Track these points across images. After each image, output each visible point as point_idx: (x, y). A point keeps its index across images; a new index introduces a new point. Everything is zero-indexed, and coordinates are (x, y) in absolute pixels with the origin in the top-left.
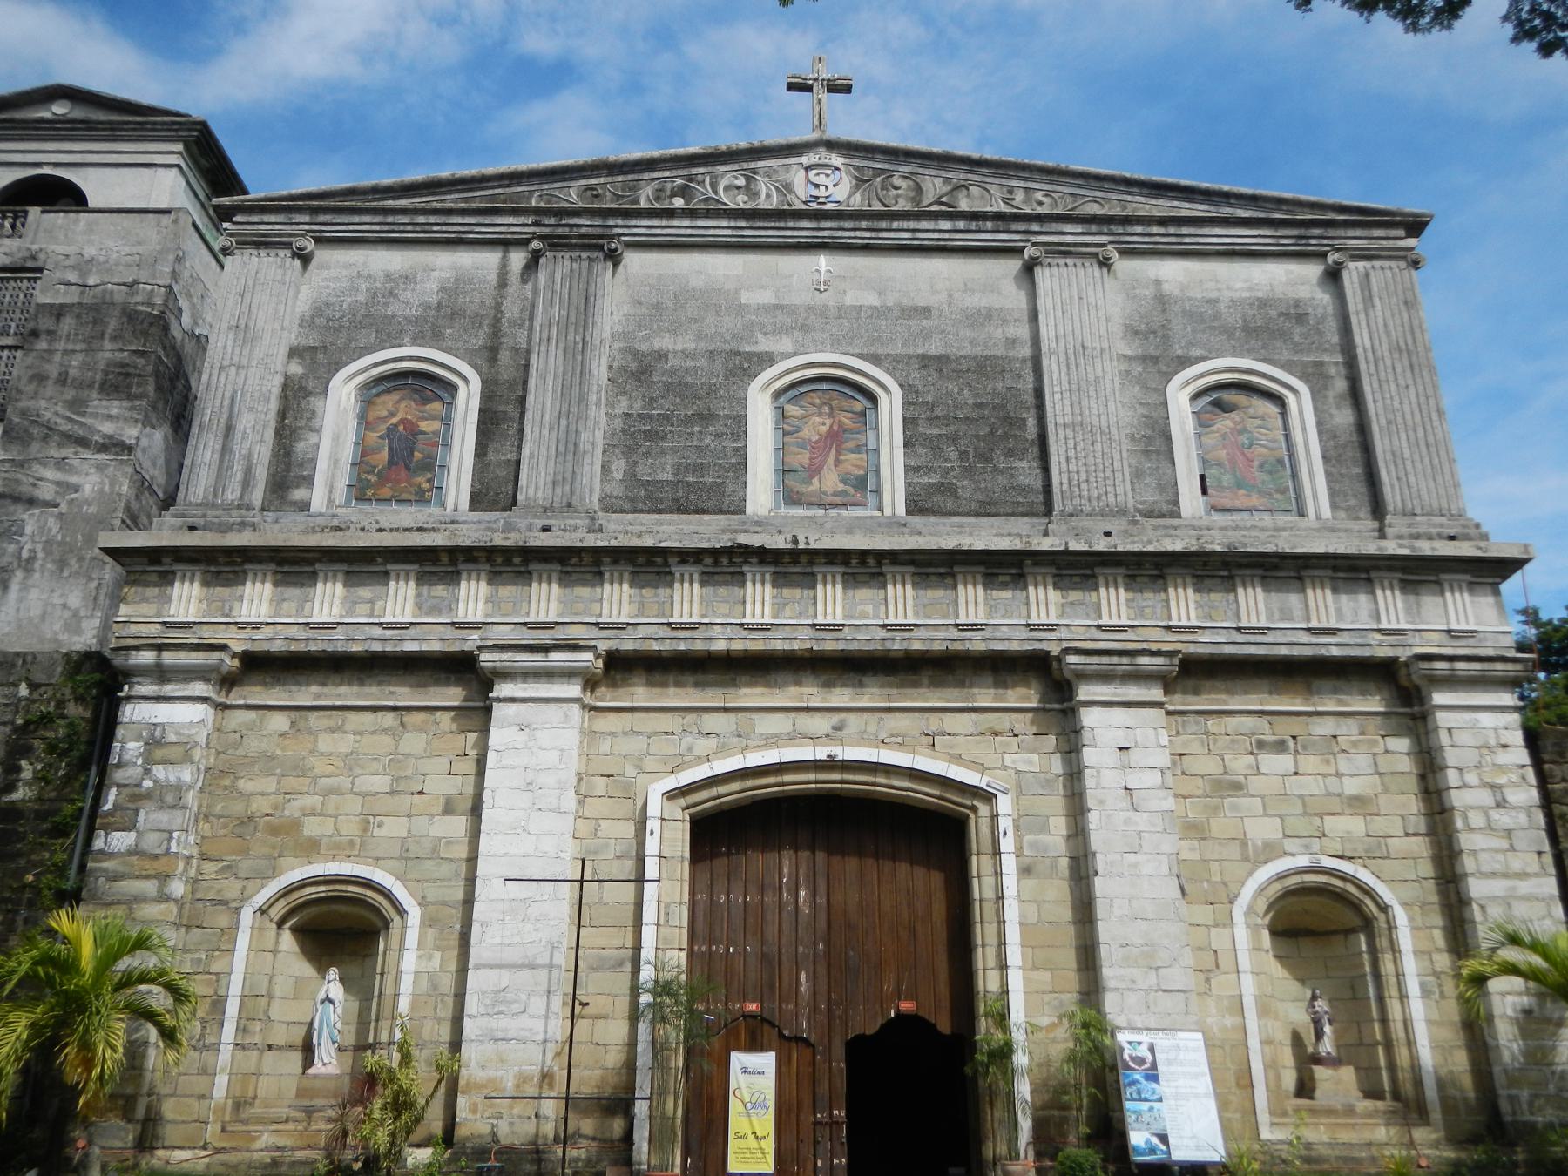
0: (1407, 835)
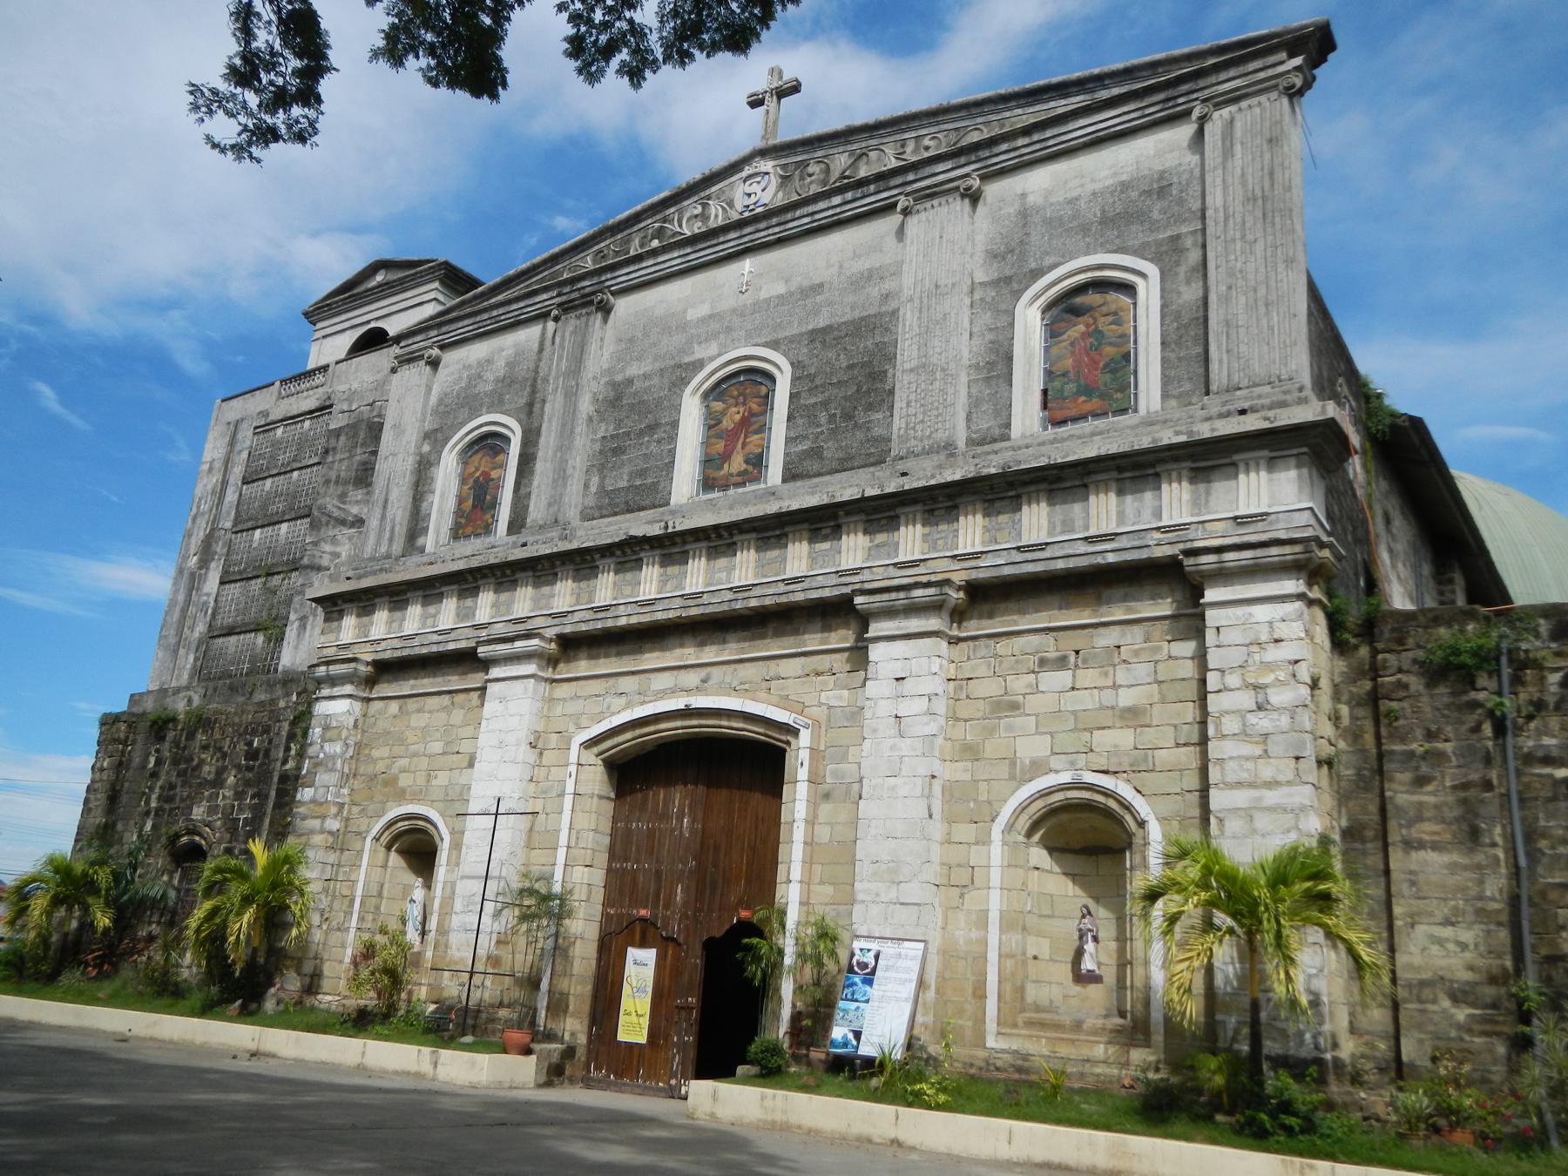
0: (1178, 745)
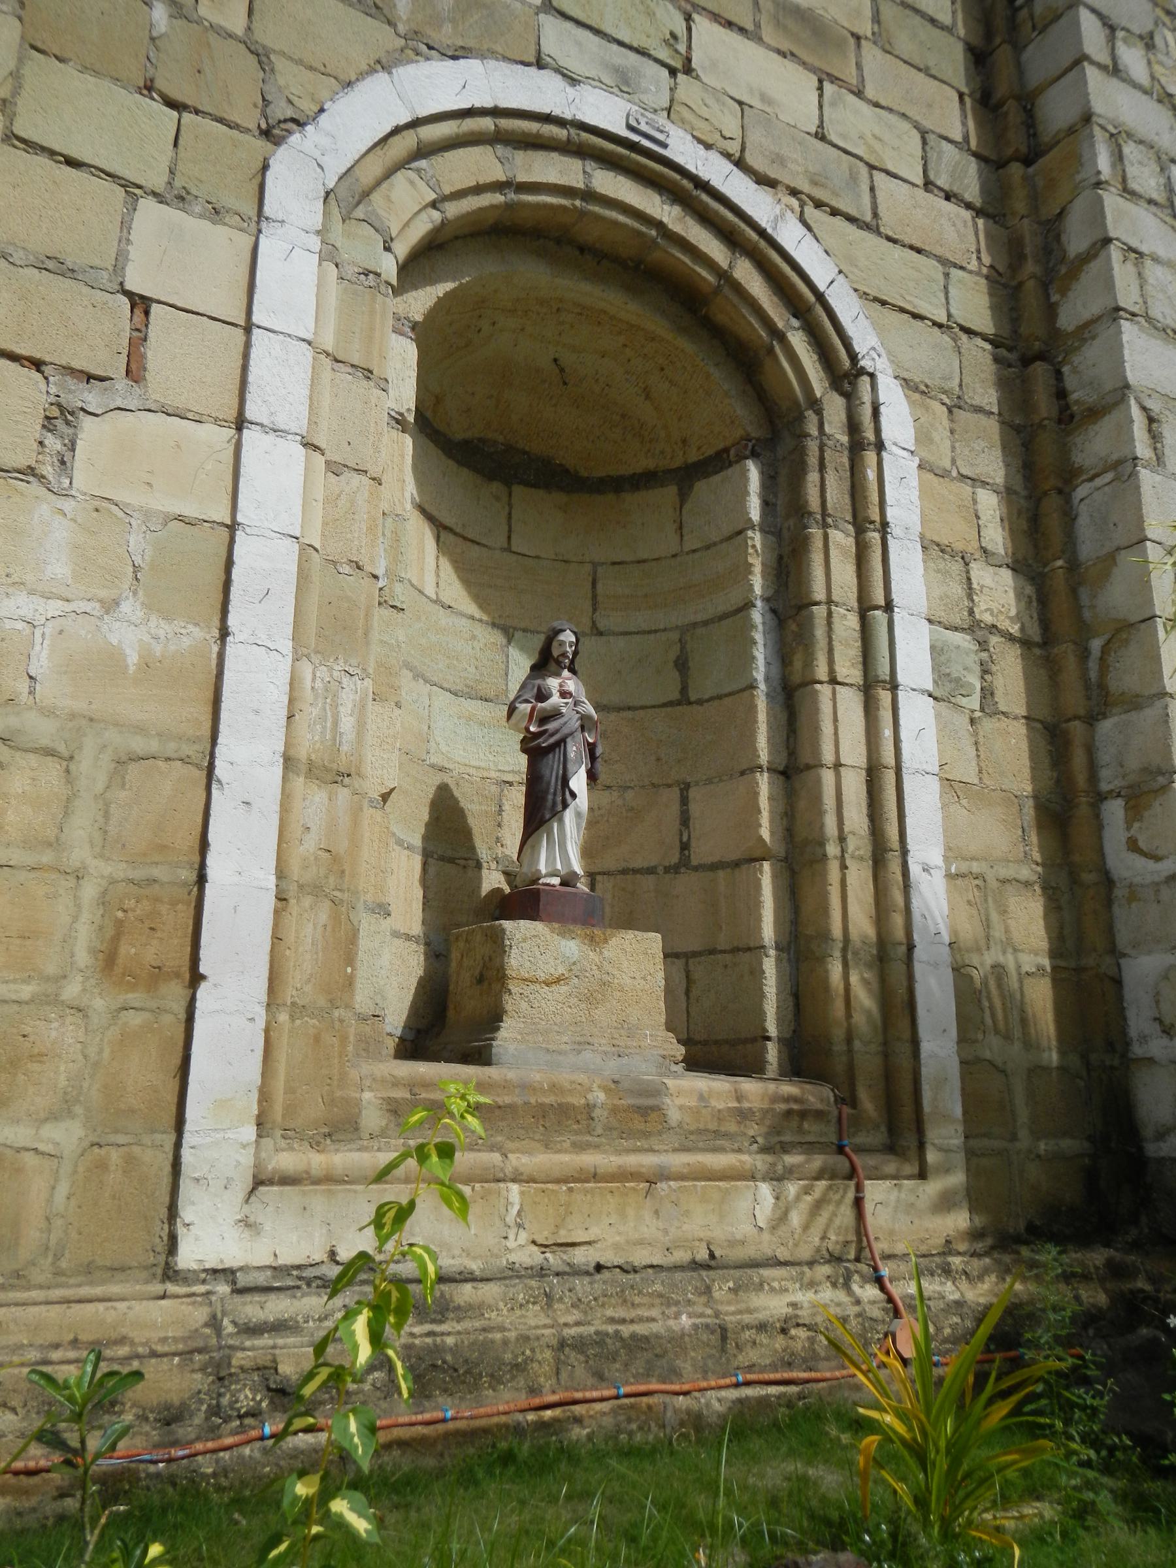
0: (928, 185)
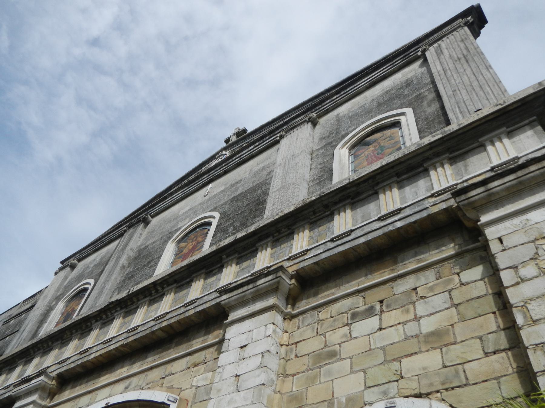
0: (487, 354)
